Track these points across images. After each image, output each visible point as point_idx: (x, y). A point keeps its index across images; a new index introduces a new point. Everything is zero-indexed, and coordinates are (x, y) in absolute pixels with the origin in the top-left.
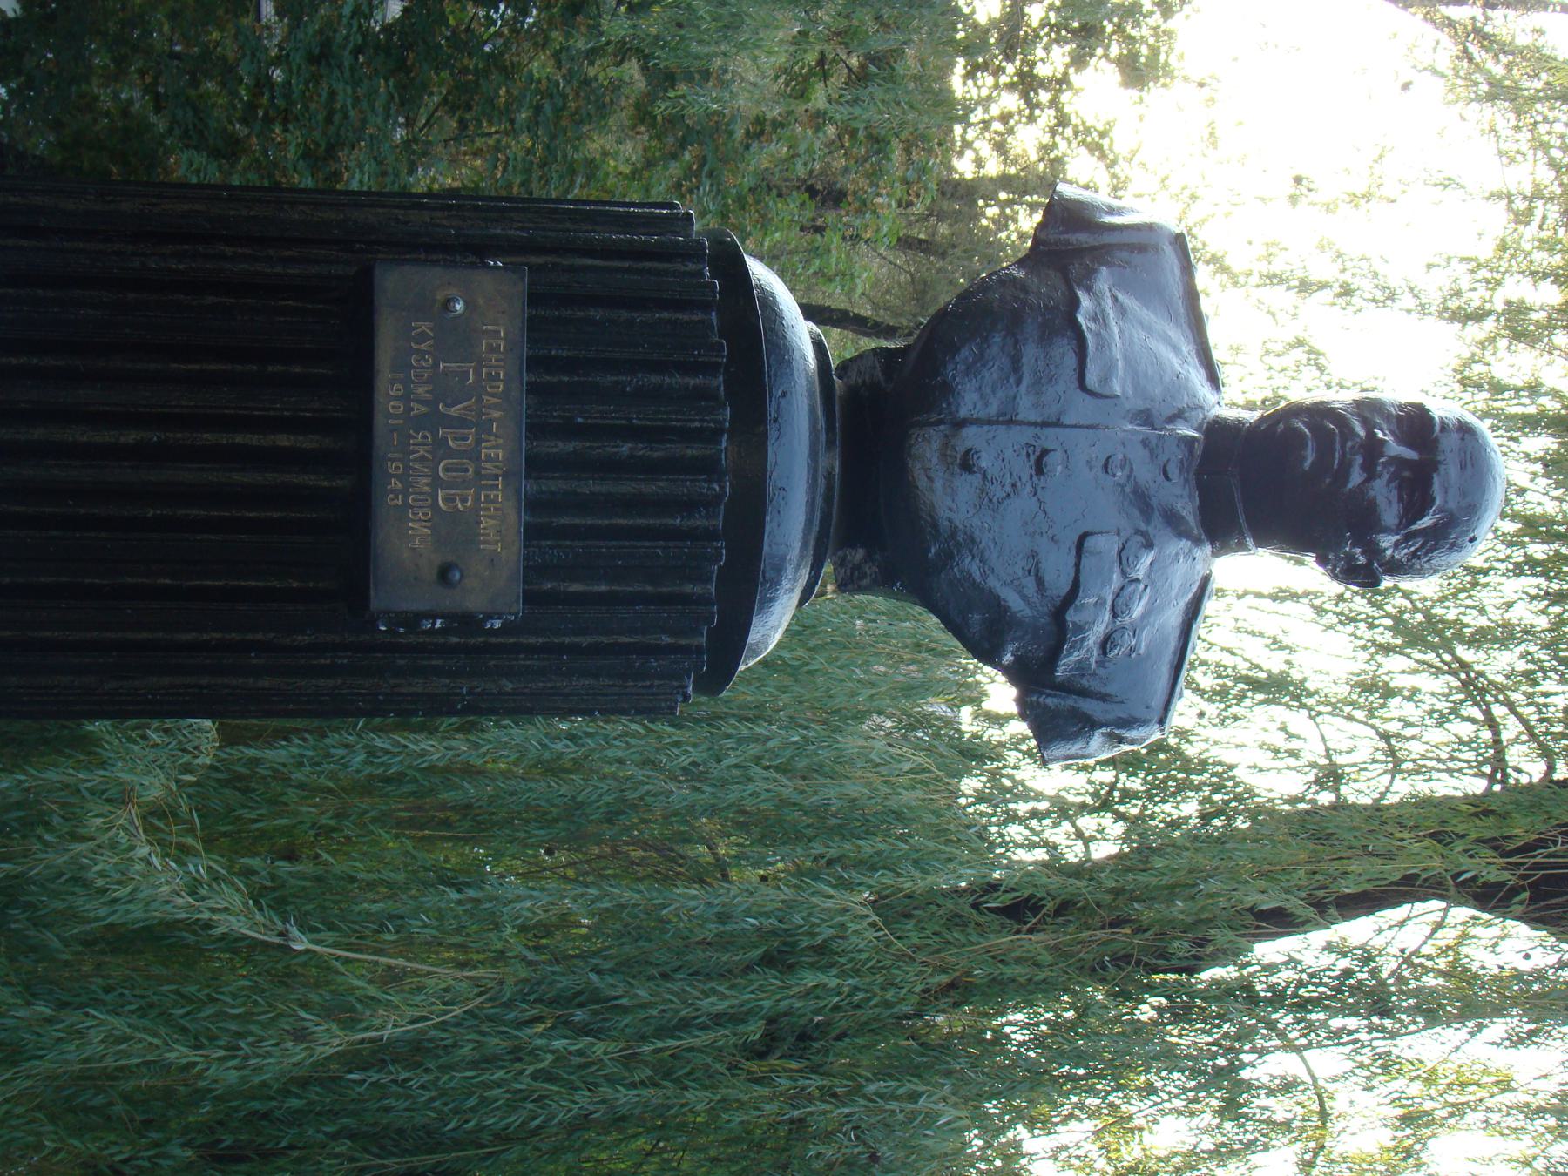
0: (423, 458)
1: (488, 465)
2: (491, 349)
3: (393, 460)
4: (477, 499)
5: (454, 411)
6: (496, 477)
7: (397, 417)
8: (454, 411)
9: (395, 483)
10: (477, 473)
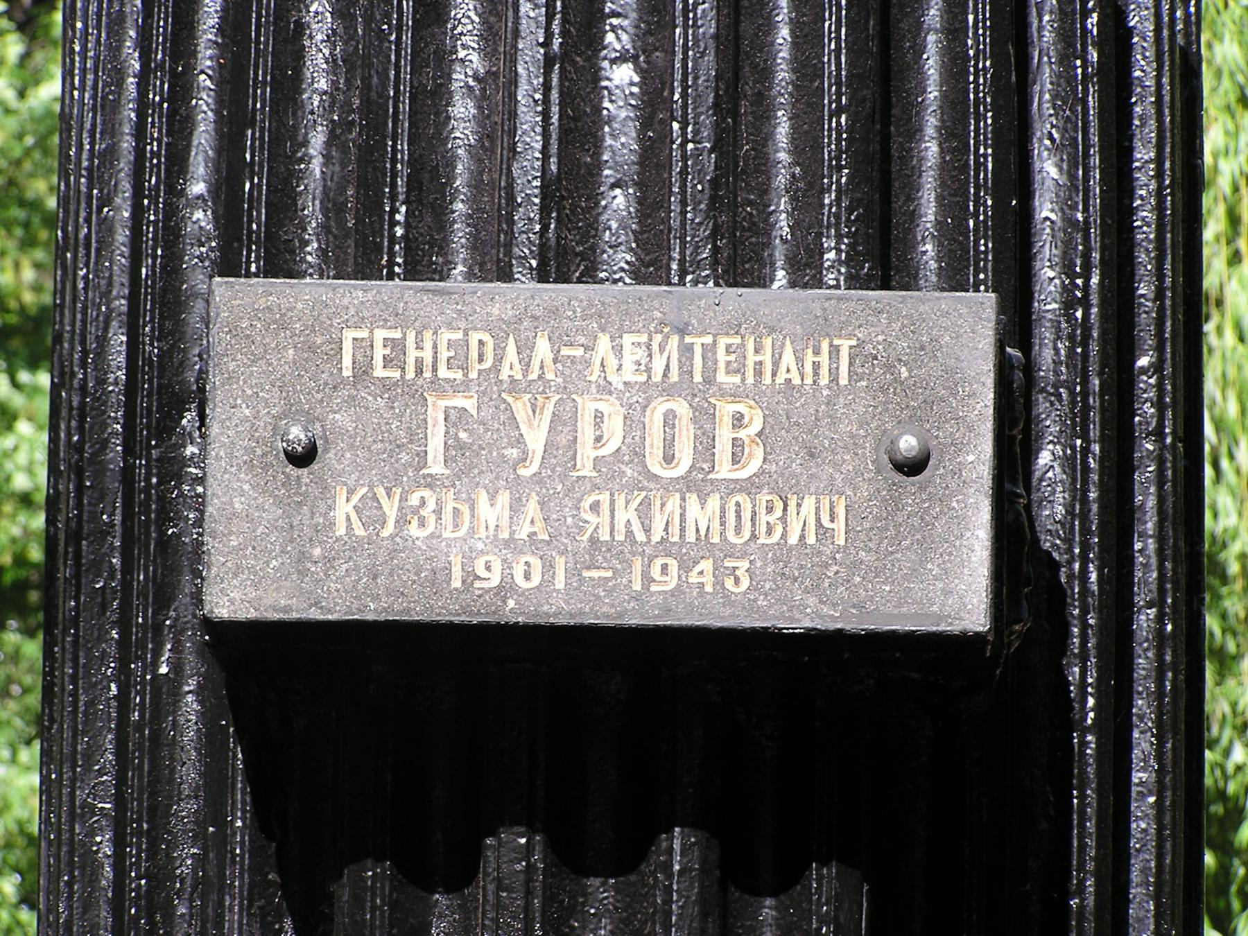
0: (644, 511)
1: (658, 365)
3: (648, 579)
4: (735, 395)
5: (536, 439)
6: (687, 350)
7: (549, 567)
8: (536, 439)
10: (669, 391)
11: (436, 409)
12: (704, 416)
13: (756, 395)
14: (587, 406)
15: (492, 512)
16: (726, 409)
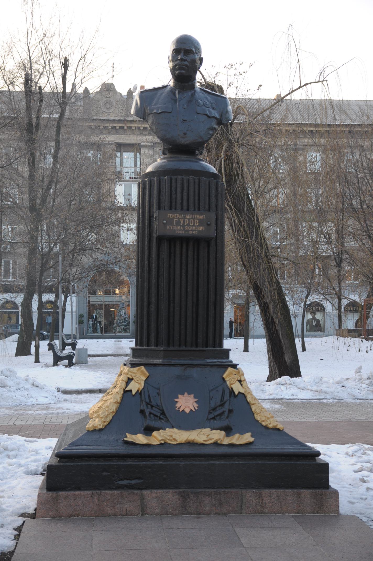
2: (172, 216)
5: (182, 222)
8: (182, 222)
9: (194, 232)
10: (192, 219)
11: (175, 220)
12: (194, 221)
13: (198, 219)
14: (186, 220)
15: (179, 227)
16: (196, 220)
